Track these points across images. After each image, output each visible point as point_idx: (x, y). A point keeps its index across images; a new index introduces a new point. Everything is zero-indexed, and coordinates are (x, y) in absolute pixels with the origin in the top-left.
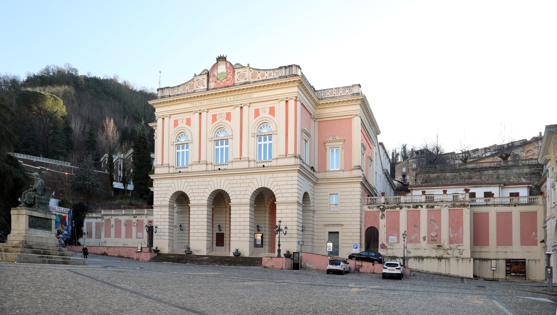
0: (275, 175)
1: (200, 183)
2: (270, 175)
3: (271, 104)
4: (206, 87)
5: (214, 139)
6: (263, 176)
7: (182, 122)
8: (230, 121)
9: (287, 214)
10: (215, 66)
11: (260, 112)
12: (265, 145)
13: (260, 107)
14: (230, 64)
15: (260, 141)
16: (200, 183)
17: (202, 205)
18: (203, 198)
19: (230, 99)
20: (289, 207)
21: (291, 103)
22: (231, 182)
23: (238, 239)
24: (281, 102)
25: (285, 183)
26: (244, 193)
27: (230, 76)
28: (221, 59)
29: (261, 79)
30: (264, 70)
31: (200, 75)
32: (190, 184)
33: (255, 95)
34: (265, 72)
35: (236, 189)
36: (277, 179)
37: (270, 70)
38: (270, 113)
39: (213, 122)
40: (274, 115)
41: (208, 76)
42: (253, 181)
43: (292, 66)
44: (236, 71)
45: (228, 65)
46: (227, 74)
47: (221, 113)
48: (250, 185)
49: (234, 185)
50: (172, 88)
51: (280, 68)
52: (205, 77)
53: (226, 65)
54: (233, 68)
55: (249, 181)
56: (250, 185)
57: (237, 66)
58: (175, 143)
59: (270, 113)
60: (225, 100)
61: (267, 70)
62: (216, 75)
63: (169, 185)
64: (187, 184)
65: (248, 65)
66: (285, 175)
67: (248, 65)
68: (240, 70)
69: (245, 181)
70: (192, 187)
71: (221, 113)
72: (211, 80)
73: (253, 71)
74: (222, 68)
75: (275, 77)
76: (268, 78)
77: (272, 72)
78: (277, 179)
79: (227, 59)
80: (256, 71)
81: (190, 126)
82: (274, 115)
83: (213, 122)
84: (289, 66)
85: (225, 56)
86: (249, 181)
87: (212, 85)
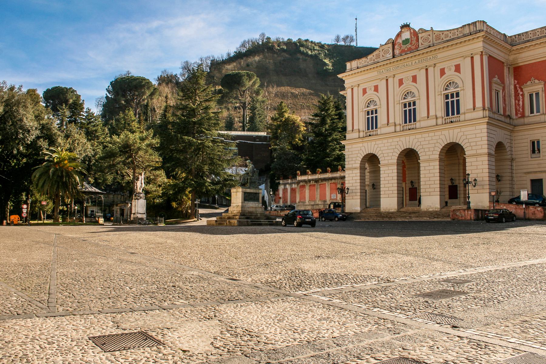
0: (463, 130)
3: (456, 62)
4: (391, 54)
7: (371, 89)
8: (416, 83)
9: (478, 167)
10: (399, 35)
11: (446, 71)
13: (446, 66)
14: (414, 30)
17: (392, 164)
18: (393, 157)
21: (477, 59)
24: (466, 59)
25: (474, 136)
28: (406, 26)
29: (445, 39)
31: (386, 44)
33: (440, 56)
37: (454, 30)
38: (456, 71)
43: (476, 22)
44: (420, 36)
45: (412, 31)
48: (439, 141)
52: (390, 45)
54: (415, 34)
59: (456, 71)
60: (410, 64)
66: (474, 128)
67: (432, 28)
68: (423, 34)
75: (459, 35)
76: (452, 37)
79: (411, 26)
80: (441, 33)
85: (408, 23)
87: (397, 52)
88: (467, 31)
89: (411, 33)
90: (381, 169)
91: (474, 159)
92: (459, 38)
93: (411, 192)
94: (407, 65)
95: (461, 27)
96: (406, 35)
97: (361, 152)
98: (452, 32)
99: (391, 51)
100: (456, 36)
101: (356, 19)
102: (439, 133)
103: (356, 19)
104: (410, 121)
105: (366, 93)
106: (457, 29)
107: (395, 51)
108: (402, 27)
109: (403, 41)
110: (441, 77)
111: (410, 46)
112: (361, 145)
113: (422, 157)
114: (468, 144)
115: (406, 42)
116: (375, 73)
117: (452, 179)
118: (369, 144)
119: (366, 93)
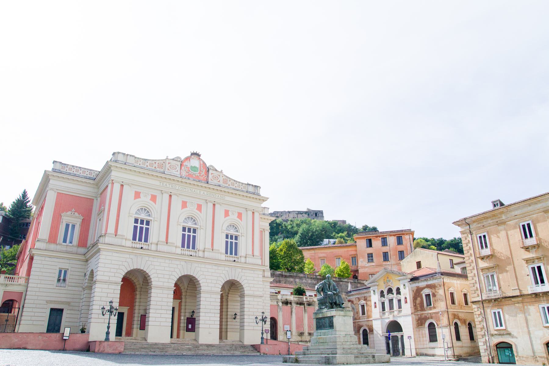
4: (179, 173)
10: (188, 159)
12: (231, 243)
14: (204, 162)
19: (204, 193)
23: (208, 326)
26: (215, 282)
27: (203, 173)
28: (196, 155)
30: (235, 181)
37: (239, 182)
43: (258, 186)
44: (211, 172)
45: (202, 163)
50: (136, 158)
52: (179, 164)
60: (198, 191)
65: (222, 171)
67: (222, 171)
68: (214, 172)
72: (183, 167)
74: (195, 162)
88: (251, 189)
89: (200, 164)
92: (243, 191)
94: (195, 191)
95: (246, 184)
96: (195, 162)
99: (179, 168)
100: (240, 189)
104: (140, 240)
105: (139, 197)
106: (243, 183)
108: (193, 154)
109: (191, 166)
111: (199, 175)
112: (128, 256)
115: (194, 168)
116: (157, 183)
117: (193, 312)
119: (139, 197)
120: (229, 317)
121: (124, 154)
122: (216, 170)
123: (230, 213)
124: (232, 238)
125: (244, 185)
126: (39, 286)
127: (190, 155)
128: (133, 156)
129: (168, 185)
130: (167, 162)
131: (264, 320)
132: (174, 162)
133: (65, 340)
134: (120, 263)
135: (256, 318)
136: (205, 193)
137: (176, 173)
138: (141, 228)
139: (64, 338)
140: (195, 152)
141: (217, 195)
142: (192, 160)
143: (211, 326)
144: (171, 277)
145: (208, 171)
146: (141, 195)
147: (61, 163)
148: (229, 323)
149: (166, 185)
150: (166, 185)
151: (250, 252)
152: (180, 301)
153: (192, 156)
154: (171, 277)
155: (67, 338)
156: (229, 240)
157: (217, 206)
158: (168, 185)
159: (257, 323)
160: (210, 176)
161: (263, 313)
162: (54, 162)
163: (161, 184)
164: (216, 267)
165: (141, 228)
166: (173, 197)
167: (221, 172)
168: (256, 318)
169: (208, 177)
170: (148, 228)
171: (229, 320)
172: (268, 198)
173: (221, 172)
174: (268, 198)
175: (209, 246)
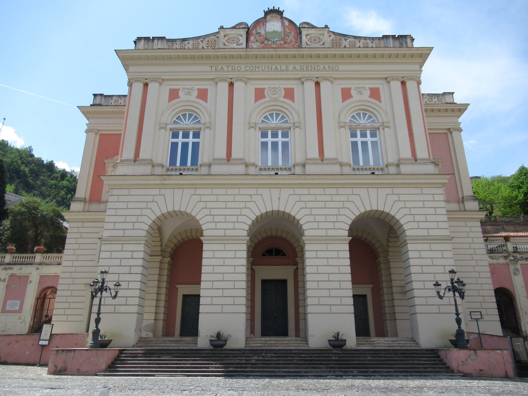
1: (231, 198)
2: (389, 191)
3: (375, 84)
4: (244, 46)
5: (258, 126)
6: (373, 191)
7: (189, 93)
10: (258, 22)
12: (364, 144)
13: (353, 87)
14: (291, 22)
15: (354, 135)
16: (231, 198)
17: (234, 239)
19: (295, 68)
20: (434, 247)
22: (303, 198)
23: (327, 309)
25: (420, 204)
26: (334, 219)
27: (291, 37)
32: (204, 198)
33: (341, 67)
34: (357, 41)
35: (314, 212)
36: (402, 198)
37: (365, 38)
38: (371, 96)
39: (257, 100)
40: (379, 100)
41: (247, 33)
42: (351, 198)
43: (405, 36)
44: (304, 32)
45: (287, 23)
46: (285, 35)
47: (275, 88)
48: (347, 205)
49: (309, 205)
50: (169, 40)
51: (385, 37)
52: (243, 32)
53: (283, 23)
55: (345, 198)
56: (347, 205)
57: (307, 26)
58: (169, 127)
59: (371, 96)
60: (284, 67)
61: (360, 38)
62: (263, 32)
63: (150, 198)
64: (197, 198)
66: (418, 191)
68: (311, 31)
69: (335, 198)
70: (209, 205)
71: (275, 88)
72: (252, 38)
73: (333, 36)
74: (274, 26)
77: (368, 41)
78: (402, 198)
80: (342, 38)
81: (206, 102)
82: (379, 100)
83: (257, 100)
84: (401, 37)
86: (345, 198)
90: (205, 247)
91: (426, 247)
93: (275, 302)
95: (379, 38)
97: (153, 206)
98: (362, 41)
99: (243, 40)
101: (4, 119)
102: (349, 191)
103: (4, 119)
105: (178, 97)
106: (373, 39)
107: (250, 44)
110: (343, 101)
111: (282, 42)
112: (156, 192)
113: (310, 230)
114: (411, 218)
116: (207, 68)
118: (178, 192)
120: (395, 290)
121: (148, 38)
122: (313, 27)
123: (353, 92)
124: (364, 135)
125: (375, 42)
126: (75, 264)
127: (262, 15)
128: (162, 38)
129: (225, 69)
130: (222, 33)
131: (457, 288)
132: (235, 31)
133: (43, 346)
134: (144, 205)
135: (437, 284)
136: (298, 67)
137: (240, 47)
138: (185, 146)
139: (41, 343)
140: (271, 8)
141: (322, 67)
142: (268, 24)
143: (334, 309)
144: (241, 219)
145: (300, 33)
146: (181, 93)
147: (102, 95)
148: (396, 303)
149: (222, 68)
150: (222, 68)
151: (407, 154)
152: (295, 267)
153: (269, 17)
154: (241, 219)
155: (46, 343)
156: (359, 139)
157: (323, 85)
158: (225, 69)
159: (441, 297)
160: (304, 38)
161: (452, 272)
162: (95, 95)
163: (214, 69)
164: (333, 191)
165: (185, 146)
166: (236, 85)
167: (326, 27)
168: (437, 284)
169: (301, 41)
170: (198, 143)
171: (396, 296)
172: (431, 49)
173: (326, 27)
174: (431, 49)
175: (314, 153)
